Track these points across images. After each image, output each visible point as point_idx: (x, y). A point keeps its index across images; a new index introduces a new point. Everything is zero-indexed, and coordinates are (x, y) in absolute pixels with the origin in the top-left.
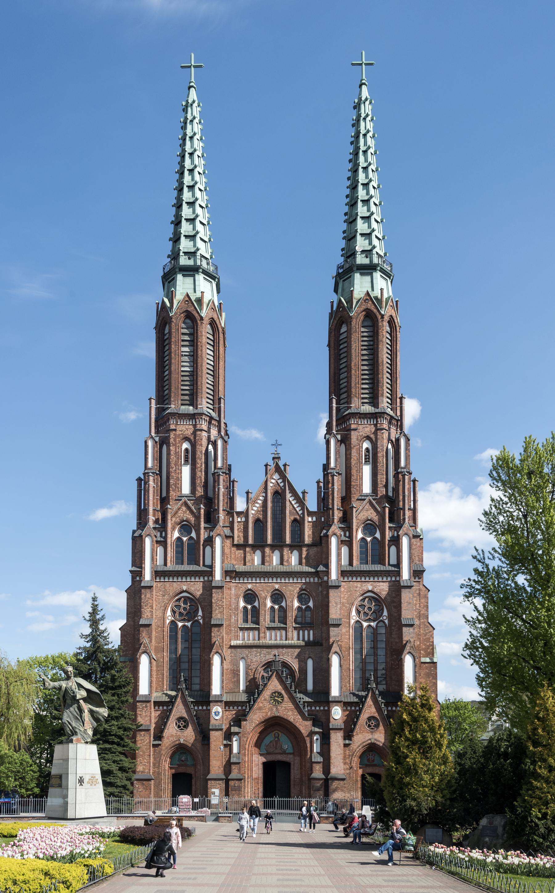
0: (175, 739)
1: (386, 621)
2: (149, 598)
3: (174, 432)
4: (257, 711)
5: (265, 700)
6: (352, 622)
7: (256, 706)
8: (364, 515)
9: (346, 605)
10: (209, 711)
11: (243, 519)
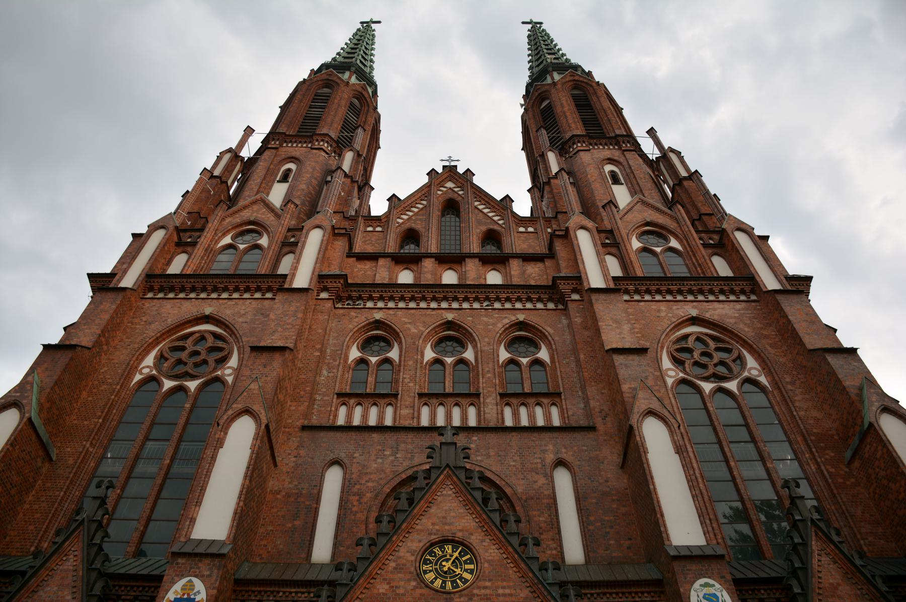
1: (763, 380)
5: (399, 569)
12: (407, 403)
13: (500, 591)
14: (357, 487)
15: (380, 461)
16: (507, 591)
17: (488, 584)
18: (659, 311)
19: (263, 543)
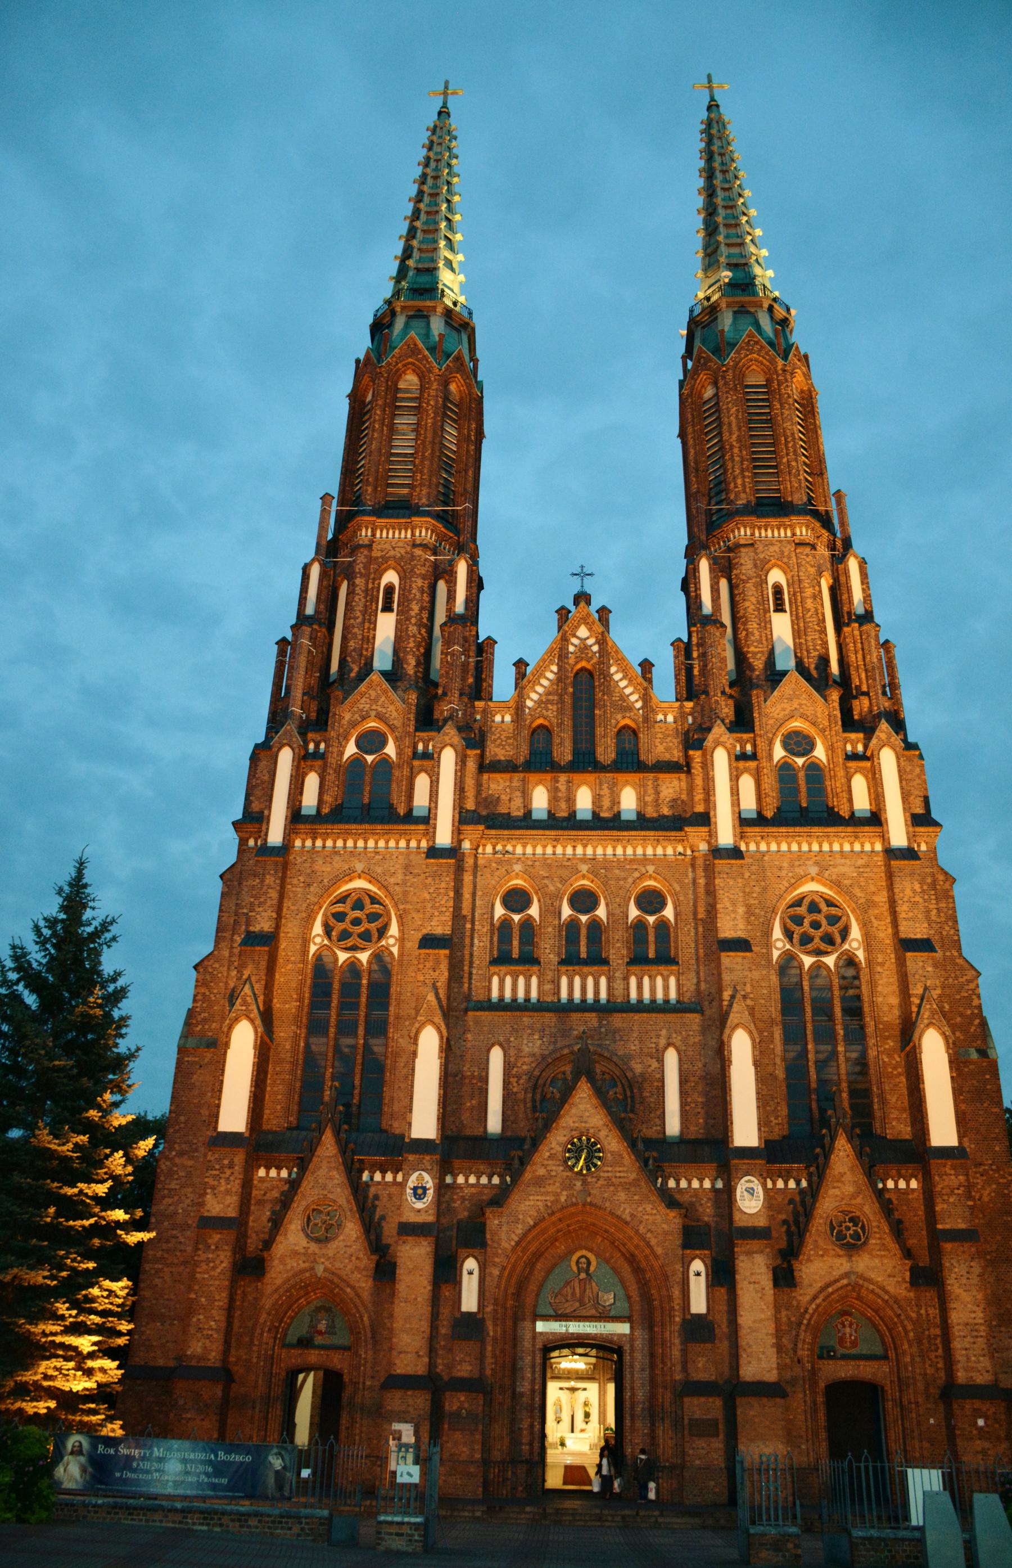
0: (303, 1265)
1: (861, 955)
2: (269, 887)
3: (366, 552)
4: (533, 1189)
5: (551, 1157)
6: (776, 954)
7: (528, 1176)
8: (784, 710)
9: (757, 911)
10: (402, 1185)
11: (508, 718)
12: (549, 978)
13: (618, 1175)
14: (515, 1069)
15: (530, 1044)
16: (622, 1175)
17: (610, 1169)
18: (780, 868)
19: (452, 1119)
